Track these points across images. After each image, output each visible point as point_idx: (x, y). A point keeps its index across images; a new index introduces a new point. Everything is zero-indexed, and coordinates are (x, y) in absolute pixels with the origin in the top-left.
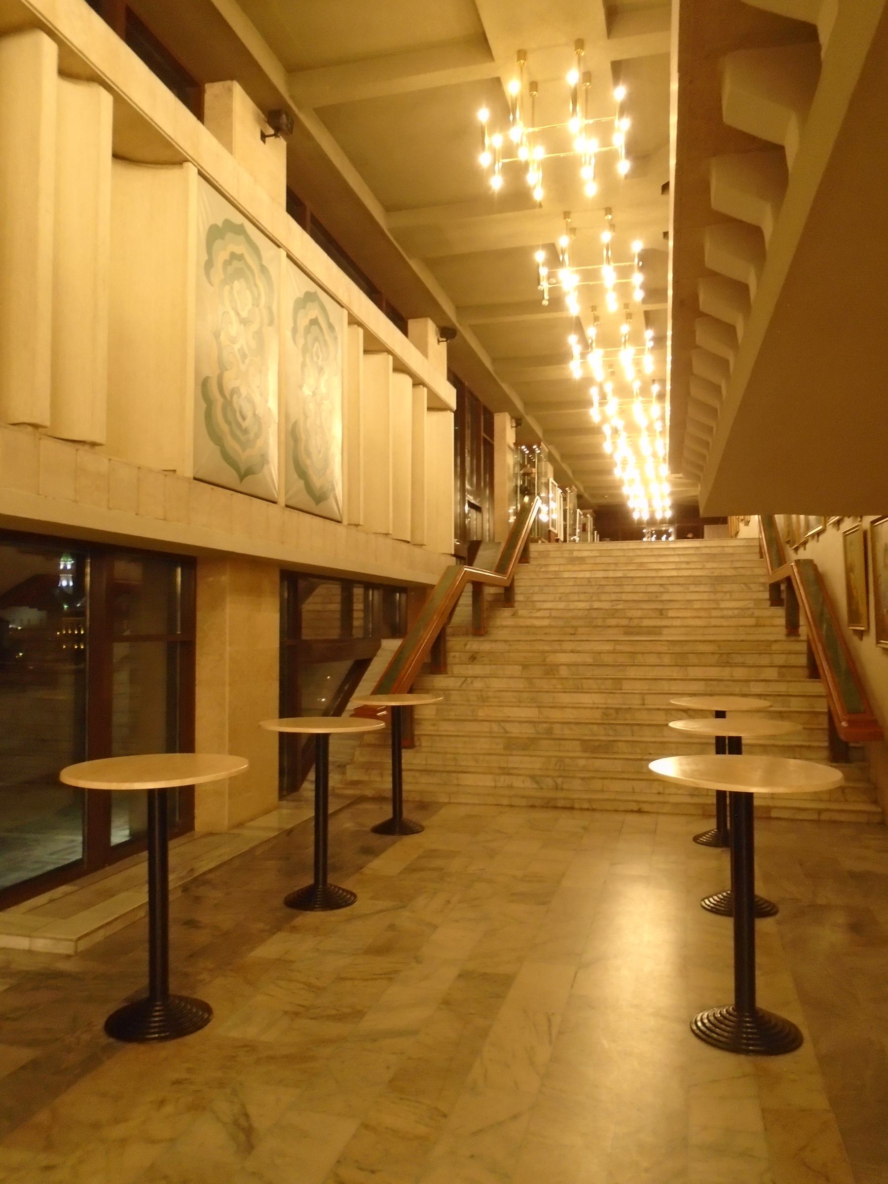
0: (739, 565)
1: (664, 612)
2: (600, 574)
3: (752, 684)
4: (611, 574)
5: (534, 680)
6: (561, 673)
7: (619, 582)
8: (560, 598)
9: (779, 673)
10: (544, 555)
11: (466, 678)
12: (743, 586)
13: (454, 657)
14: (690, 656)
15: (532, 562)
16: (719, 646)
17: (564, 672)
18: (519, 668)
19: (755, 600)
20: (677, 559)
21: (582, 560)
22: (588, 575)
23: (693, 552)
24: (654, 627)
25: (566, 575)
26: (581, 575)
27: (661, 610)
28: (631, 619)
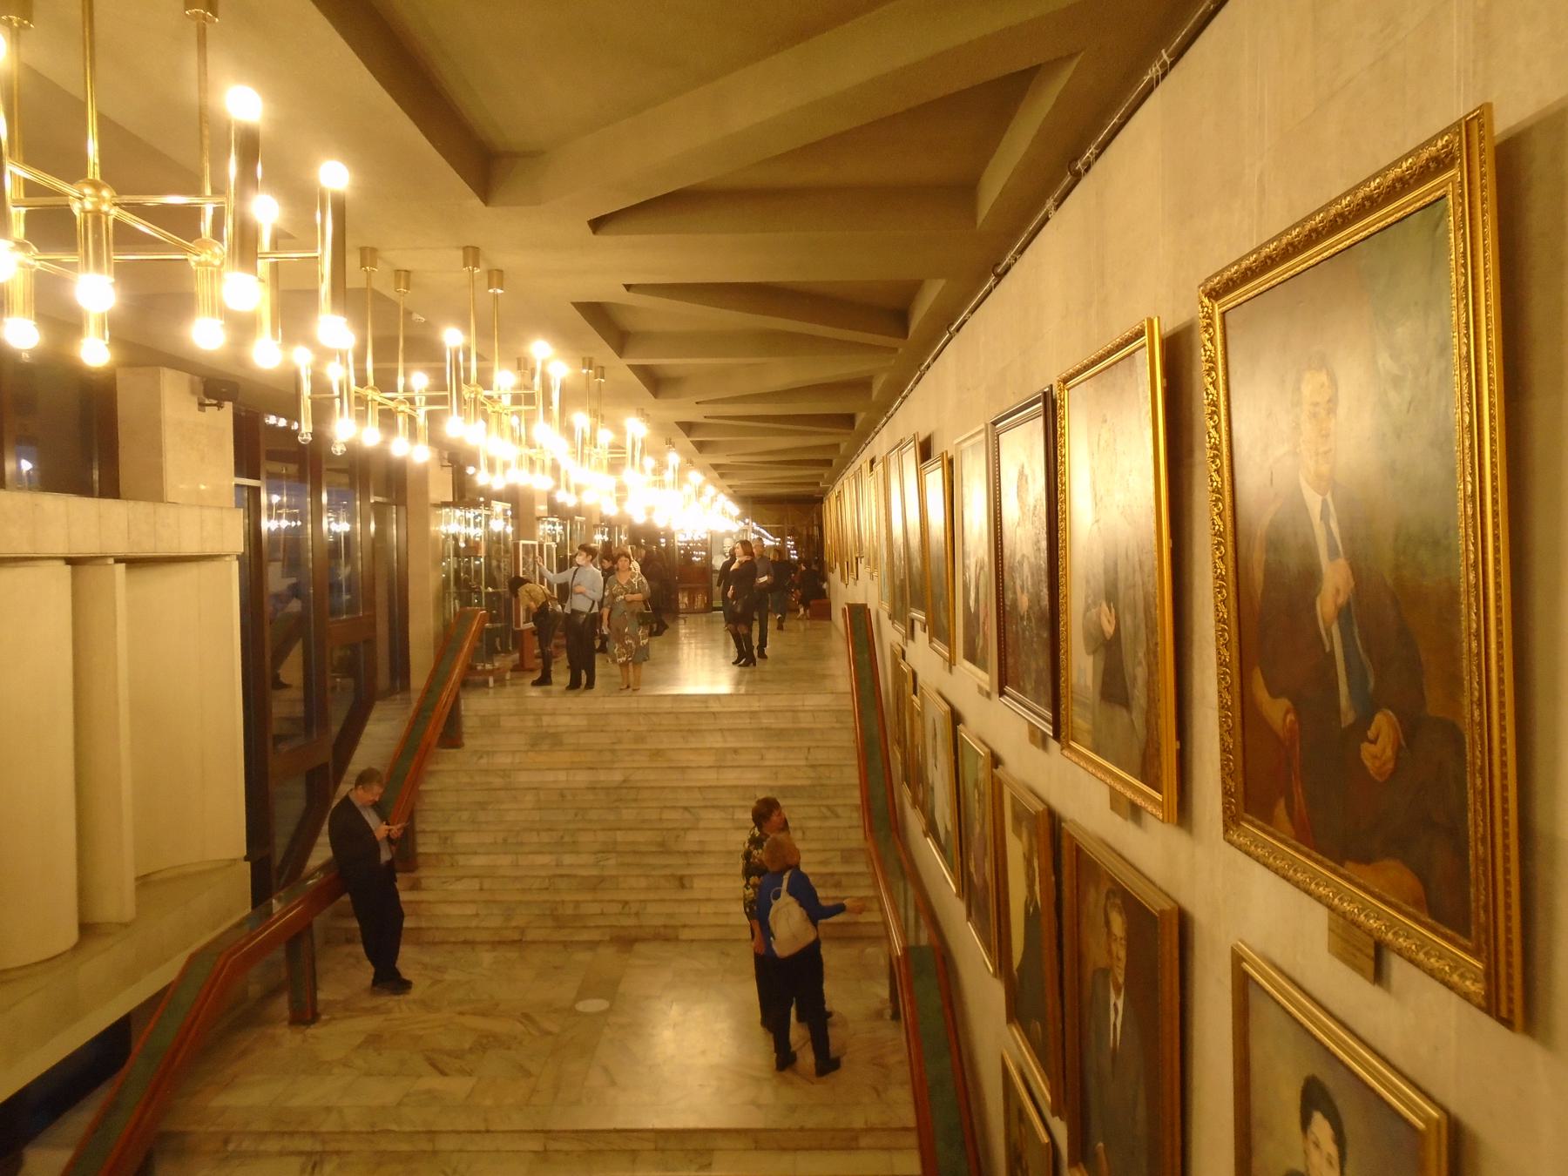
0: (820, 756)
1: (686, 882)
2: (582, 778)
4: (602, 776)
8: (505, 840)
10: (491, 724)
12: (824, 810)
15: (468, 743)
16: (756, 1142)
19: (843, 851)
20: (716, 742)
21: (554, 740)
24: (665, 926)
25: (523, 778)
26: (550, 777)
27: (681, 878)
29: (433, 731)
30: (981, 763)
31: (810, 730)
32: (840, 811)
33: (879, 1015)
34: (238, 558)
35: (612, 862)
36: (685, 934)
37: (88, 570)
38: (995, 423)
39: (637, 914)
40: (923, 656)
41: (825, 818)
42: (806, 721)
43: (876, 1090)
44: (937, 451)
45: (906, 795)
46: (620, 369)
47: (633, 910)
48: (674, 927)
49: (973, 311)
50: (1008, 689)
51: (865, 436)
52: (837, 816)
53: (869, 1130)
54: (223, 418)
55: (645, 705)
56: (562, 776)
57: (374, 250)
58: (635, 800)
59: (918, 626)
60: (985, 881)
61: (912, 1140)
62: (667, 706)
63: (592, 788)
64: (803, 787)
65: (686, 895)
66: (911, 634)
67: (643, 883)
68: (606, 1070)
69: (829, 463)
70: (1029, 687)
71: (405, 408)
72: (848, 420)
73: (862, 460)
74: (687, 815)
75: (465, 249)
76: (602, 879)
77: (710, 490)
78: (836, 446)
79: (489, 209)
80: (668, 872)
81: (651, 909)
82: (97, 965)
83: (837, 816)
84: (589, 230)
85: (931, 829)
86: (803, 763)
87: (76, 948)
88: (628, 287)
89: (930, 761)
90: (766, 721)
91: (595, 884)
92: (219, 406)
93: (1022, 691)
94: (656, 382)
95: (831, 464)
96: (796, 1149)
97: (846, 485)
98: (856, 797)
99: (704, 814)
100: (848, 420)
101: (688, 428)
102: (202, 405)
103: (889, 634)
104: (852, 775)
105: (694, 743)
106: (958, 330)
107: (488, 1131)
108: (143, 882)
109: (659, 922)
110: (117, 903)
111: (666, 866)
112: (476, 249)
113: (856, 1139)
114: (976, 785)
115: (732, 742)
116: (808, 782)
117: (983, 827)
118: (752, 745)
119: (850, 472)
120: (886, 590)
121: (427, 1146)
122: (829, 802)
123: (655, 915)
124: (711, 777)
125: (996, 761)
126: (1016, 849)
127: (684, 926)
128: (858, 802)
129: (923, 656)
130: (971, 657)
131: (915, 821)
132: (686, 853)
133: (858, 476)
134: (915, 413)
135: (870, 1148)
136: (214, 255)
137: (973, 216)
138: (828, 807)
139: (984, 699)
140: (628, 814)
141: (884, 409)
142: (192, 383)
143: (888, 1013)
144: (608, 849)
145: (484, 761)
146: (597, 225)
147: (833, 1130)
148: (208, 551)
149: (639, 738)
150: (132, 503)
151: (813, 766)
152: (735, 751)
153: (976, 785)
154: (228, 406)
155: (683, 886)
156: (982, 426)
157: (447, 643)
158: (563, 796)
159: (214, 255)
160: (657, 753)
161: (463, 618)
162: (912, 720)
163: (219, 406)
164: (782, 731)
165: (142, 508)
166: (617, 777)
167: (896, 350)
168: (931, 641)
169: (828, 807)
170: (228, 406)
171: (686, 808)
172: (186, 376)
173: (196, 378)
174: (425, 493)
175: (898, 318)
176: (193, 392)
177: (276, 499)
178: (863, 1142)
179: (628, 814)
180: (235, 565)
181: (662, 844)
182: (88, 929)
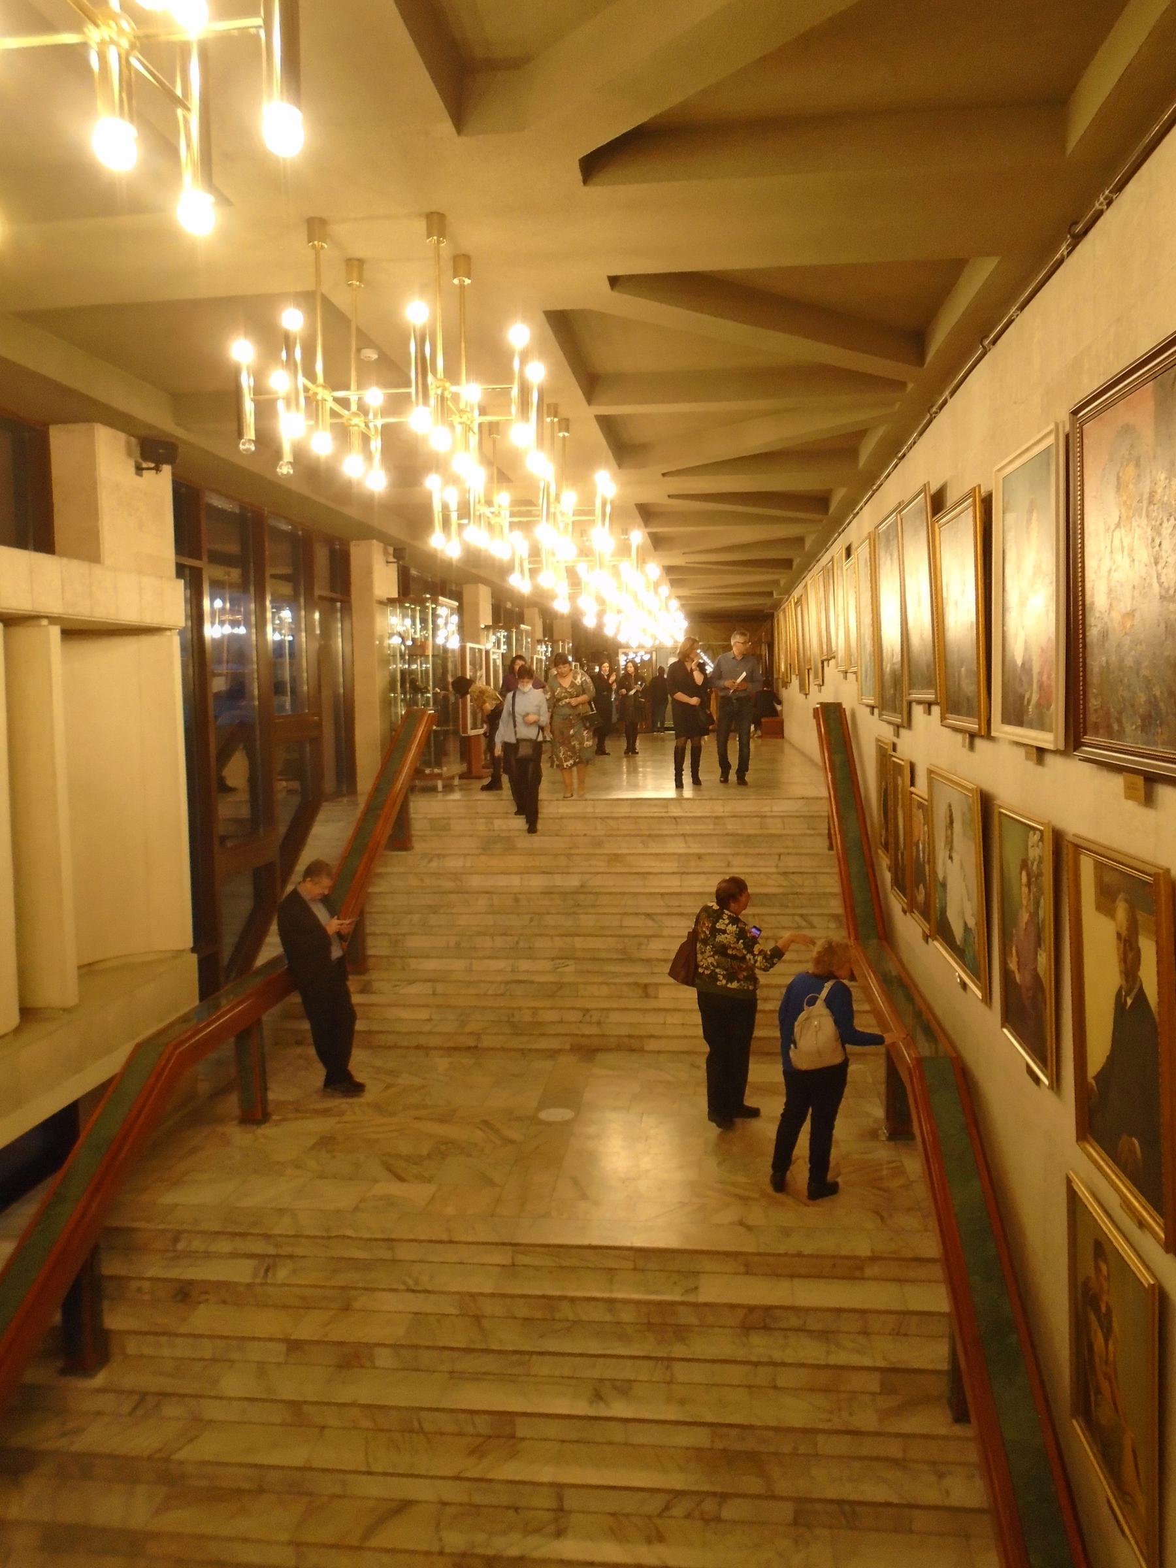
0: (791, 863)
1: (651, 991)
2: (537, 882)
3: (821, 1439)
4: (558, 881)
5: (306, 1408)
6: (379, 1363)
7: (575, 900)
8: (458, 944)
9: (882, 1385)
10: (440, 827)
11: (144, 1396)
12: (797, 918)
13: (139, 1290)
14: (682, 1310)
15: (418, 846)
16: (747, 1265)
17: (385, 1358)
18: (282, 1347)
20: (677, 847)
22: (515, 881)
23: (708, 828)
24: (630, 1036)
25: (476, 882)
26: (502, 881)
27: (646, 986)
28: (588, 1010)
29: (383, 830)
30: (1034, 838)
31: (780, 836)
32: (815, 920)
33: (873, 1135)
34: (182, 633)
35: (571, 969)
36: (652, 1045)
37: (22, 633)
38: (1075, 413)
39: (599, 1023)
40: (929, 742)
41: (799, 928)
42: (775, 827)
43: (882, 1218)
44: (951, 498)
45: (896, 904)
46: (584, 414)
47: (594, 1019)
48: (641, 1037)
49: (1022, 308)
50: (1087, 739)
51: (837, 525)
52: (813, 927)
53: (874, 1259)
54: (161, 483)
55: (601, 810)
56: (515, 881)
57: (323, 222)
58: (593, 906)
59: (918, 710)
60: (1037, 978)
61: (937, 1271)
62: (624, 810)
63: (547, 893)
64: (775, 895)
65: (653, 1004)
66: (909, 724)
67: (605, 991)
68: (575, 1182)
69: (787, 563)
70: (1129, 729)
71: (358, 421)
72: (820, 502)
73: (837, 549)
74: (650, 923)
75: (429, 216)
76: (561, 986)
77: (665, 589)
78: (800, 540)
79: (460, 140)
80: (630, 980)
81: (614, 1017)
82: (38, 1050)
83: (813, 927)
84: (578, 175)
85: (941, 930)
86: (774, 870)
87: (17, 1031)
88: (614, 281)
89: (941, 853)
90: (732, 826)
91: (555, 990)
92: (157, 469)
93: (1110, 734)
94: (624, 446)
95: (788, 564)
96: (792, 1276)
97: (811, 588)
98: (836, 906)
99: (667, 921)
100: (820, 502)
101: (647, 513)
102: (139, 469)
103: (871, 731)
104: (831, 883)
105: (654, 848)
106: (994, 342)
107: (451, 1242)
108: (87, 970)
109: (624, 1031)
110: (59, 987)
111: (628, 975)
112: (442, 216)
113: (861, 1269)
114: (1025, 865)
115: (695, 848)
116: (780, 890)
117: (1034, 915)
118: (716, 851)
119: (817, 568)
120: (870, 683)
121: (387, 1255)
122: (804, 911)
123: (619, 1023)
124: (673, 884)
125: (1058, 837)
126: (1100, 934)
127: (651, 1036)
128: (840, 911)
129: (929, 742)
130: (1016, 715)
131: (908, 927)
132: (649, 961)
133: (829, 573)
134: (927, 462)
135: (875, 1279)
136: (121, 31)
137: (1062, 141)
138: (802, 916)
139: (1031, 765)
140: (587, 921)
141: (869, 481)
142: (128, 445)
143: (884, 1132)
144: (566, 956)
145: (434, 864)
146: (593, 166)
147: (834, 1257)
148: (149, 620)
149: (598, 843)
150: (65, 561)
151: (785, 873)
152: (700, 857)
153: (1025, 865)
154: (167, 469)
155: (647, 996)
156: (1052, 426)
157: (394, 743)
158: (517, 900)
159: (121, 31)
160: (616, 858)
161: (412, 718)
162: (909, 818)
163: (157, 469)
164: (749, 836)
165: (76, 568)
166: (574, 882)
167: (903, 385)
168: (943, 718)
169: (802, 916)
170: (167, 469)
171: (648, 915)
172: (122, 436)
173: (133, 440)
174: (370, 588)
175: (914, 341)
176: (129, 454)
177: (218, 603)
178: (868, 1272)
179: (587, 921)
180: (176, 641)
181: (623, 951)
182: (27, 1013)
